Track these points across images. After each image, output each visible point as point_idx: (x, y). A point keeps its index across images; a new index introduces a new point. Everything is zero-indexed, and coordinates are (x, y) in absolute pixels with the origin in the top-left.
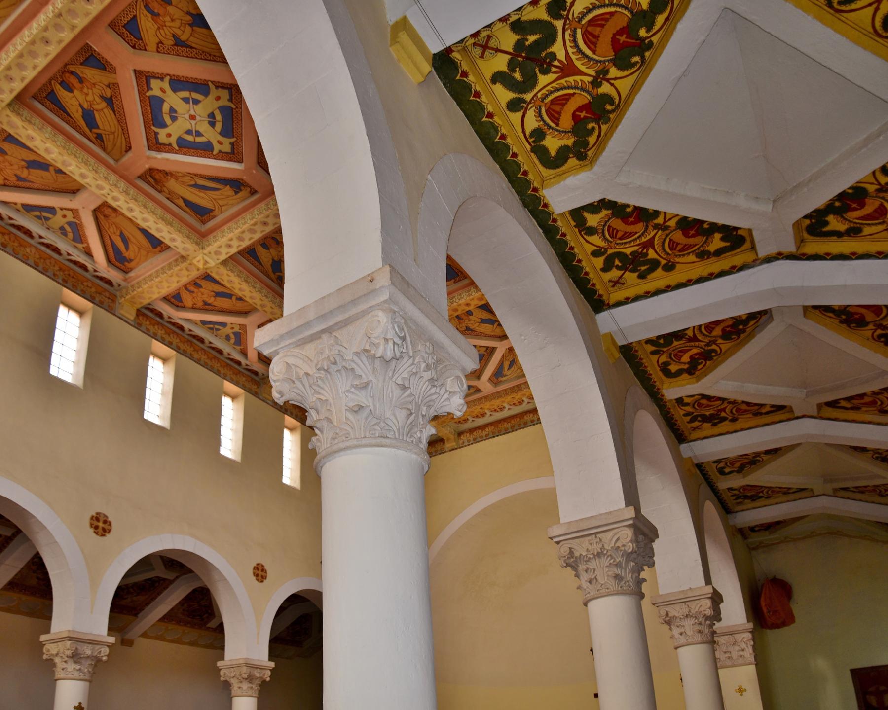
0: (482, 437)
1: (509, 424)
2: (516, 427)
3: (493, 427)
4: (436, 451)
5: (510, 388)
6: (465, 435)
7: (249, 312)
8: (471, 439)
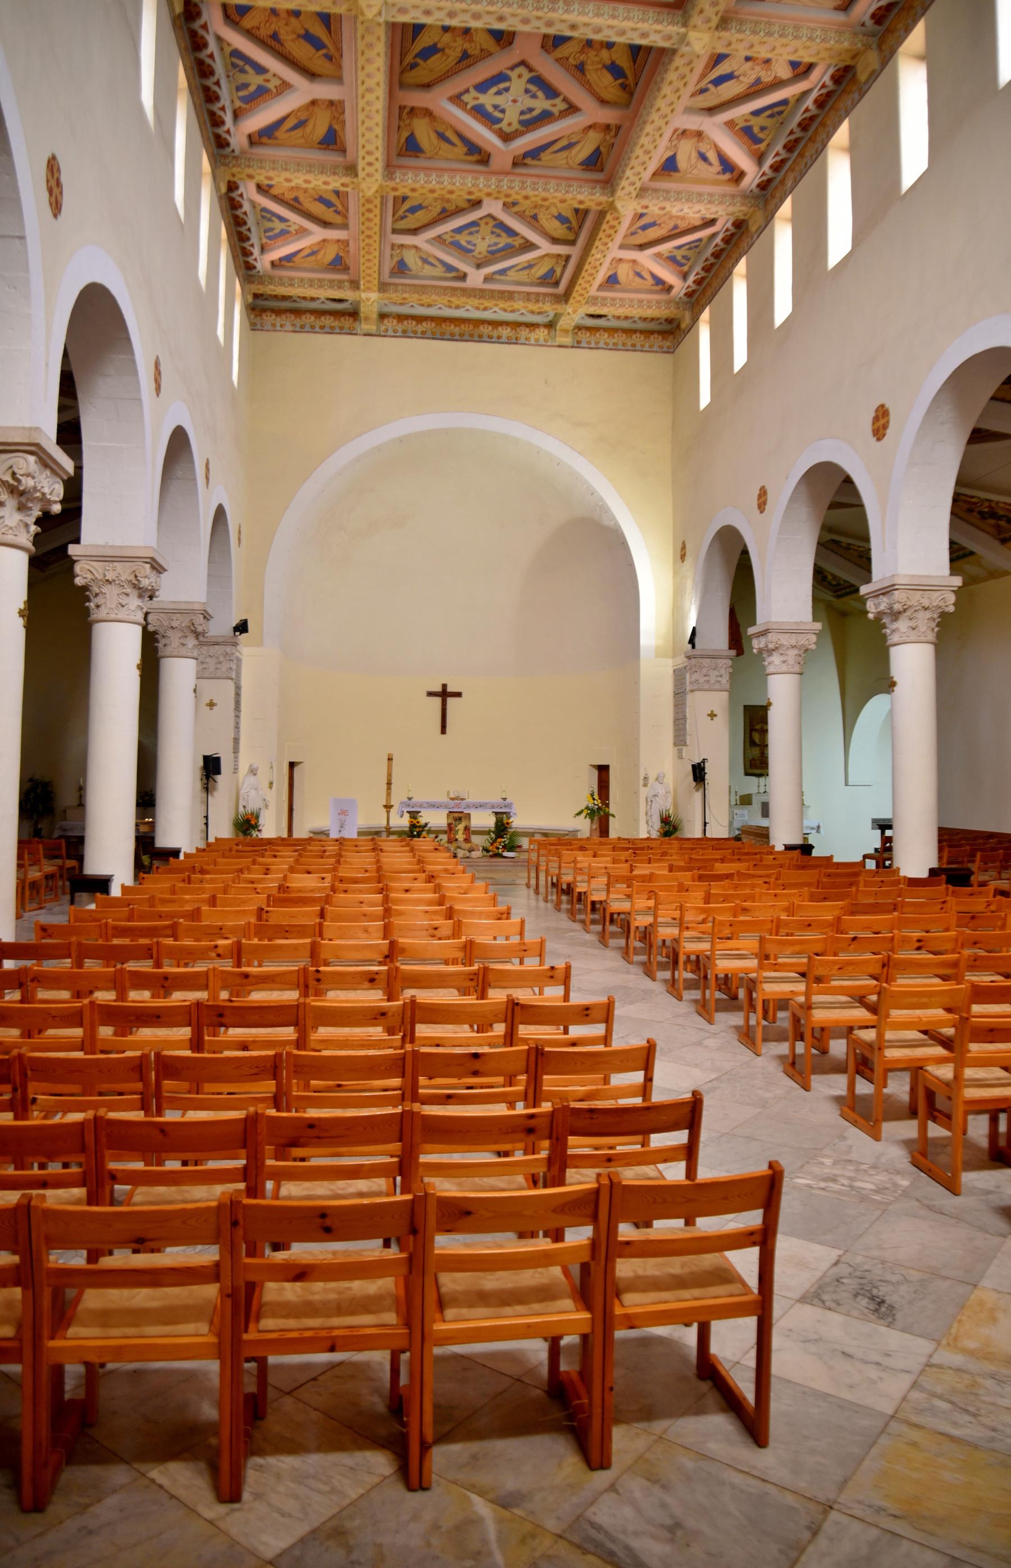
0: (415, 332)
1: (457, 329)
2: (466, 337)
3: (433, 325)
4: (342, 328)
6: (391, 320)
7: (320, 76)
8: (400, 330)
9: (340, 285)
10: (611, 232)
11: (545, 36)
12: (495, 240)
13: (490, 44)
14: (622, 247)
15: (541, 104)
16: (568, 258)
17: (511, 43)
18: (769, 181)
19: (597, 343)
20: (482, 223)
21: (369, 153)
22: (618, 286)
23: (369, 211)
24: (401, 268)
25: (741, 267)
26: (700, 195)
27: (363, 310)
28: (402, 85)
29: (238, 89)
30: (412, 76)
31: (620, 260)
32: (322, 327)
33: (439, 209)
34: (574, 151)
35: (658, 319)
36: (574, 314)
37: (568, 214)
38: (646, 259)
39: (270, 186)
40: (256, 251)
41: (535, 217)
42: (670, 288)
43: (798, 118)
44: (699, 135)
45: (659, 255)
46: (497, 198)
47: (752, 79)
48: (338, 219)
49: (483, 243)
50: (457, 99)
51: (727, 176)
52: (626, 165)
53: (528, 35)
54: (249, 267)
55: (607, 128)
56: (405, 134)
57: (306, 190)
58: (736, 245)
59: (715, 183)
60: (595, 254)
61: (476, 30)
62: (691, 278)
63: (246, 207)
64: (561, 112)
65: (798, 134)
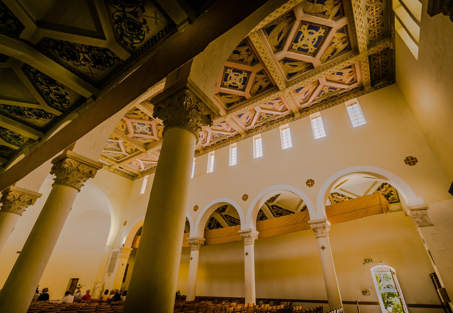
15: (147, 132)
30: (130, 116)
34: (145, 141)
35: (133, 173)
50: (132, 123)
62: (146, 169)
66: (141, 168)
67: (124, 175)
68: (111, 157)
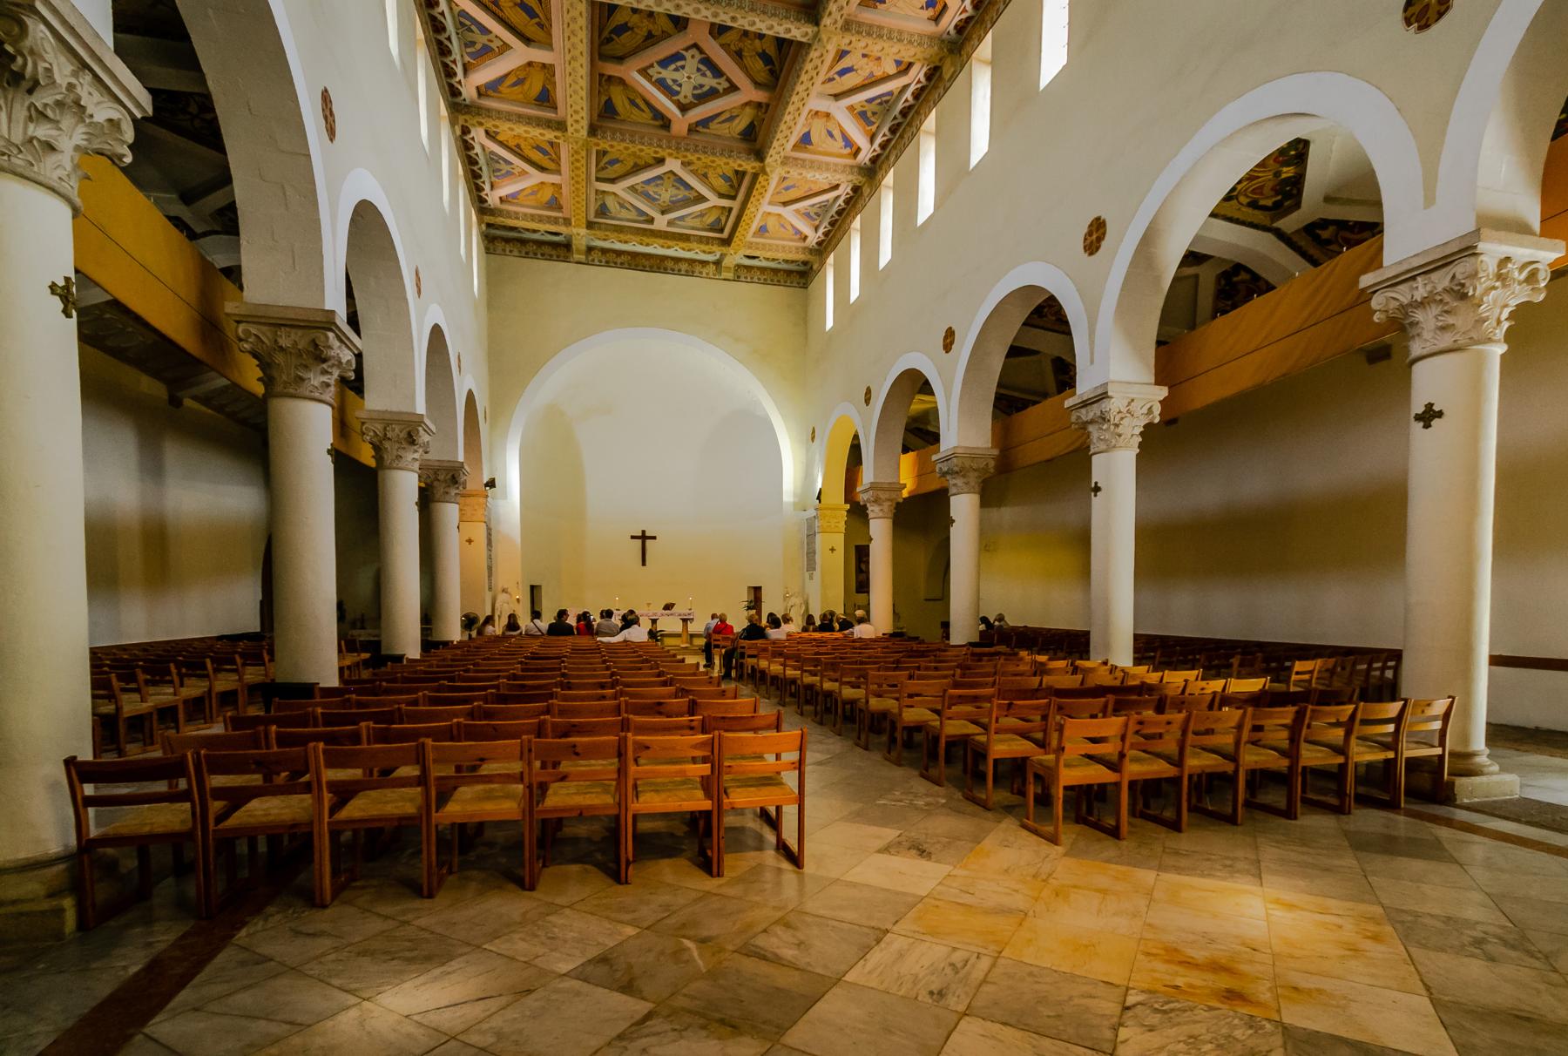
2: (655, 269)
4: (558, 256)
5: (679, 234)
9: (555, 221)
10: (763, 190)
11: (713, 24)
12: (675, 192)
13: (668, 26)
14: (770, 203)
15: (709, 82)
16: (730, 210)
17: (685, 28)
18: (878, 156)
19: (752, 278)
20: (665, 177)
21: (576, 112)
22: (767, 234)
23: (578, 161)
24: (603, 211)
25: (857, 223)
26: (828, 164)
27: (575, 243)
28: (604, 57)
29: (466, 46)
30: (608, 49)
31: (769, 213)
32: (543, 255)
33: (632, 164)
34: (737, 121)
36: (735, 256)
37: (730, 174)
38: (788, 213)
39: (497, 133)
40: (487, 187)
41: (705, 175)
42: (806, 237)
43: (900, 106)
44: (828, 115)
45: (797, 211)
46: (676, 158)
47: (866, 73)
48: (552, 166)
49: (667, 194)
50: (644, 72)
51: (848, 150)
52: (774, 137)
53: (699, 21)
54: (482, 200)
55: (759, 105)
56: (604, 98)
57: (525, 139)
58: (854, 206)
59: (841, 156)
60: (751, 207)
61: (659, 13)
62: (821, 230)
63: (478, 149)
64: (724, 89)
65: (900, 119)
66: (806, 237)
67: (772, 280)
68: (698, 229)
